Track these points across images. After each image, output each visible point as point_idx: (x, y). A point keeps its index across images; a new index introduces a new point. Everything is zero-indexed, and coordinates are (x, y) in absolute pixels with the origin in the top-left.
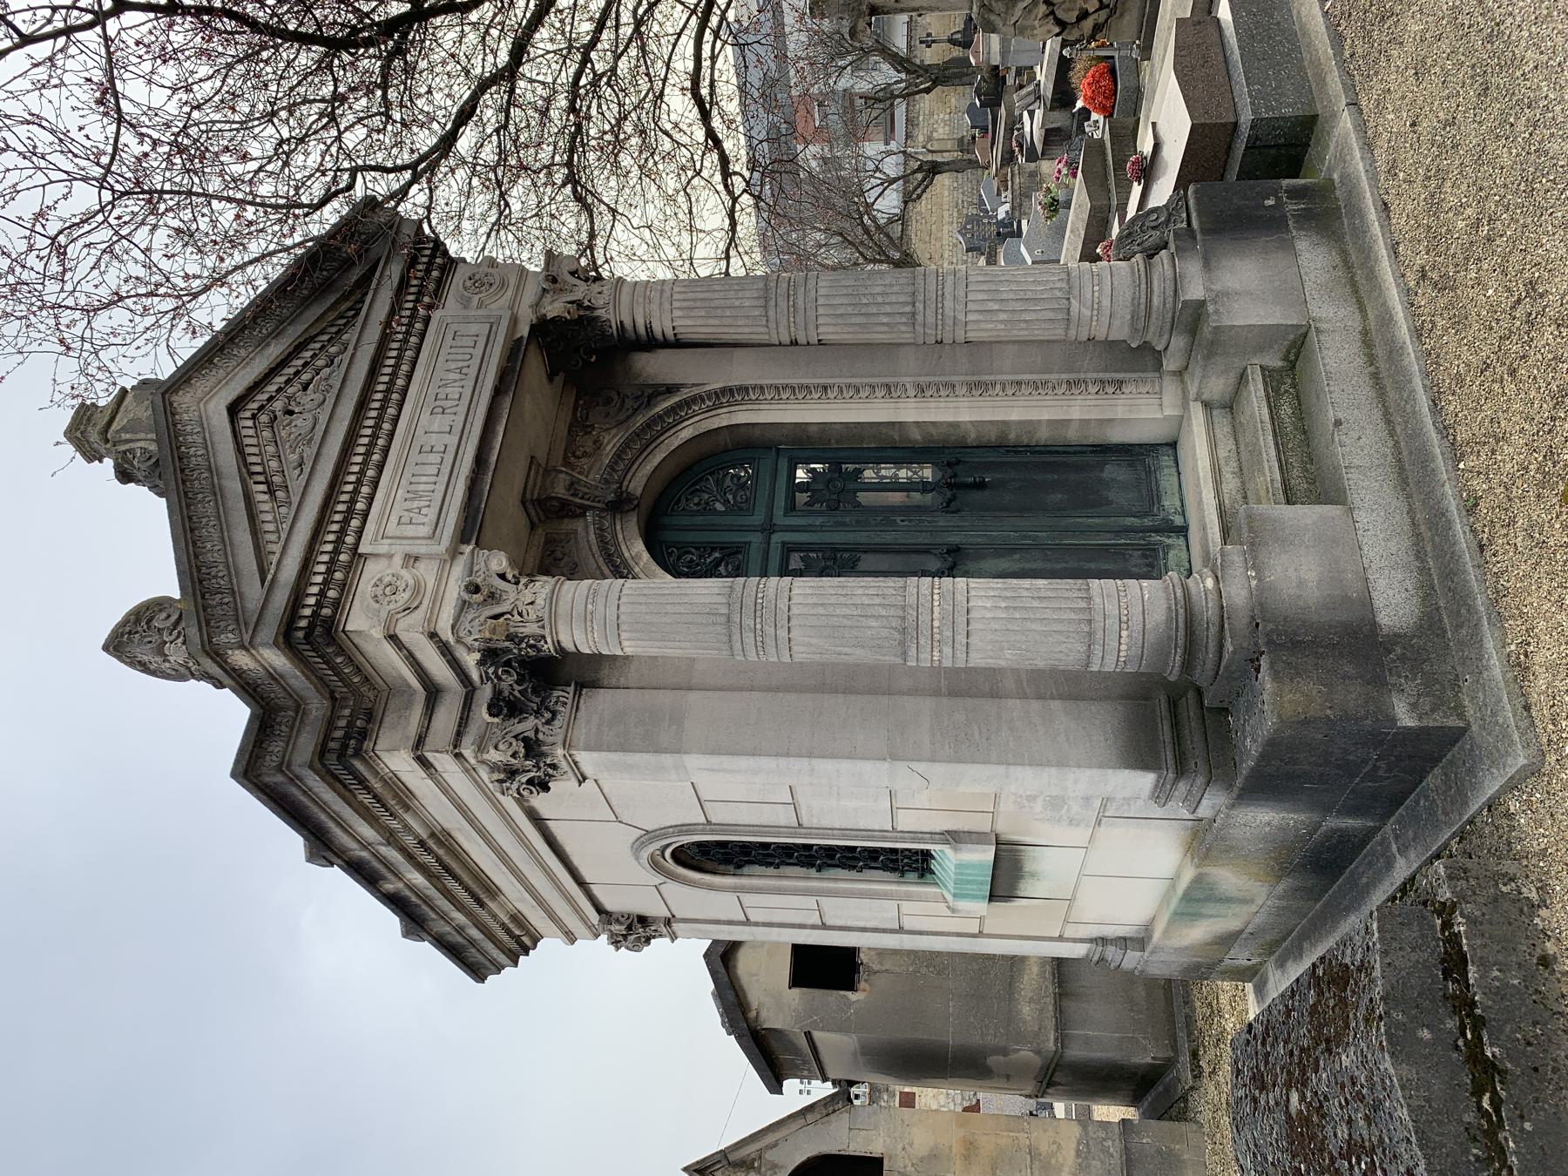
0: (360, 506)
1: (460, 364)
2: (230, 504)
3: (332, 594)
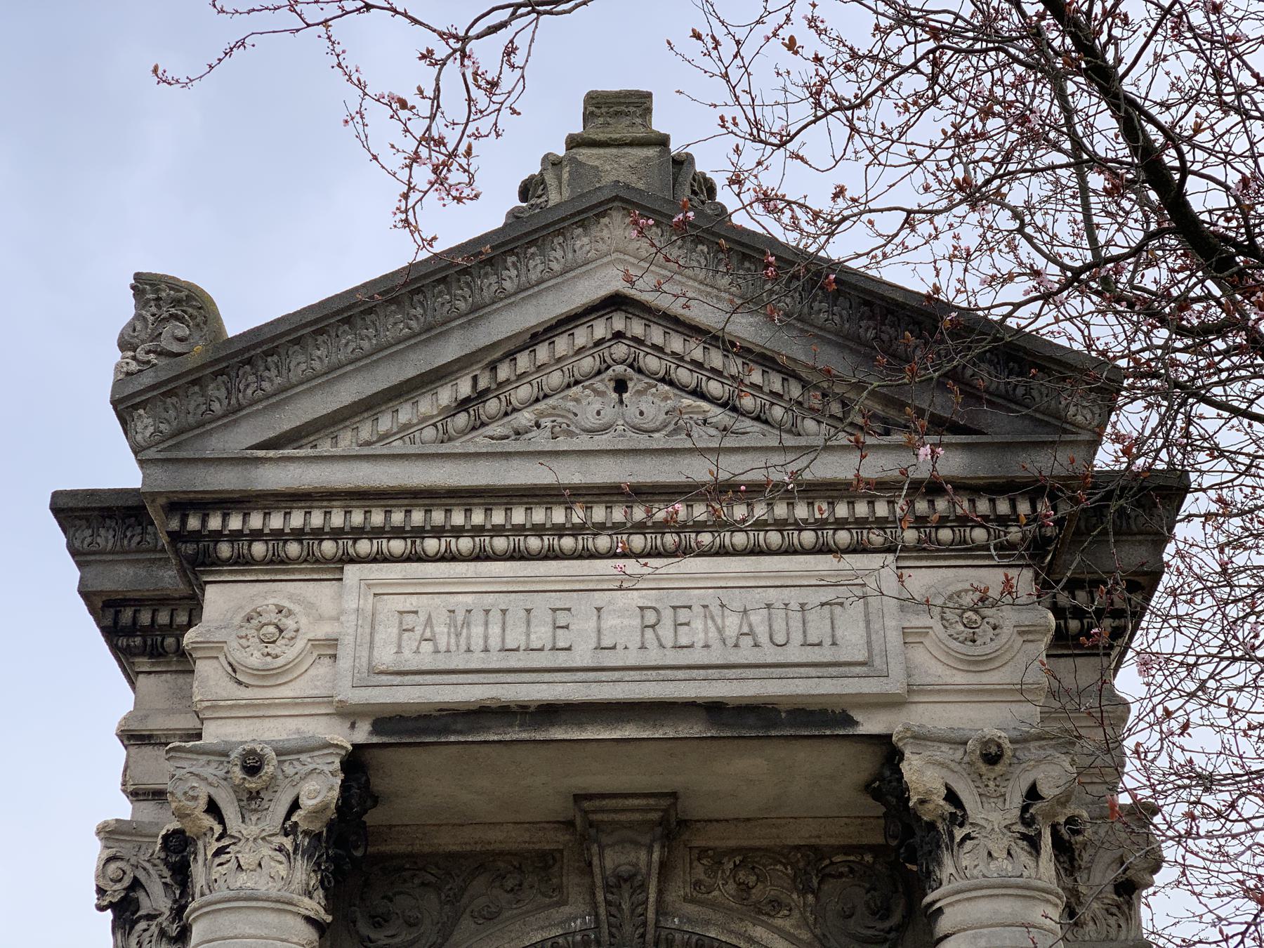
0: (431, 545)
2: (412, 356)
3: (259, 549)
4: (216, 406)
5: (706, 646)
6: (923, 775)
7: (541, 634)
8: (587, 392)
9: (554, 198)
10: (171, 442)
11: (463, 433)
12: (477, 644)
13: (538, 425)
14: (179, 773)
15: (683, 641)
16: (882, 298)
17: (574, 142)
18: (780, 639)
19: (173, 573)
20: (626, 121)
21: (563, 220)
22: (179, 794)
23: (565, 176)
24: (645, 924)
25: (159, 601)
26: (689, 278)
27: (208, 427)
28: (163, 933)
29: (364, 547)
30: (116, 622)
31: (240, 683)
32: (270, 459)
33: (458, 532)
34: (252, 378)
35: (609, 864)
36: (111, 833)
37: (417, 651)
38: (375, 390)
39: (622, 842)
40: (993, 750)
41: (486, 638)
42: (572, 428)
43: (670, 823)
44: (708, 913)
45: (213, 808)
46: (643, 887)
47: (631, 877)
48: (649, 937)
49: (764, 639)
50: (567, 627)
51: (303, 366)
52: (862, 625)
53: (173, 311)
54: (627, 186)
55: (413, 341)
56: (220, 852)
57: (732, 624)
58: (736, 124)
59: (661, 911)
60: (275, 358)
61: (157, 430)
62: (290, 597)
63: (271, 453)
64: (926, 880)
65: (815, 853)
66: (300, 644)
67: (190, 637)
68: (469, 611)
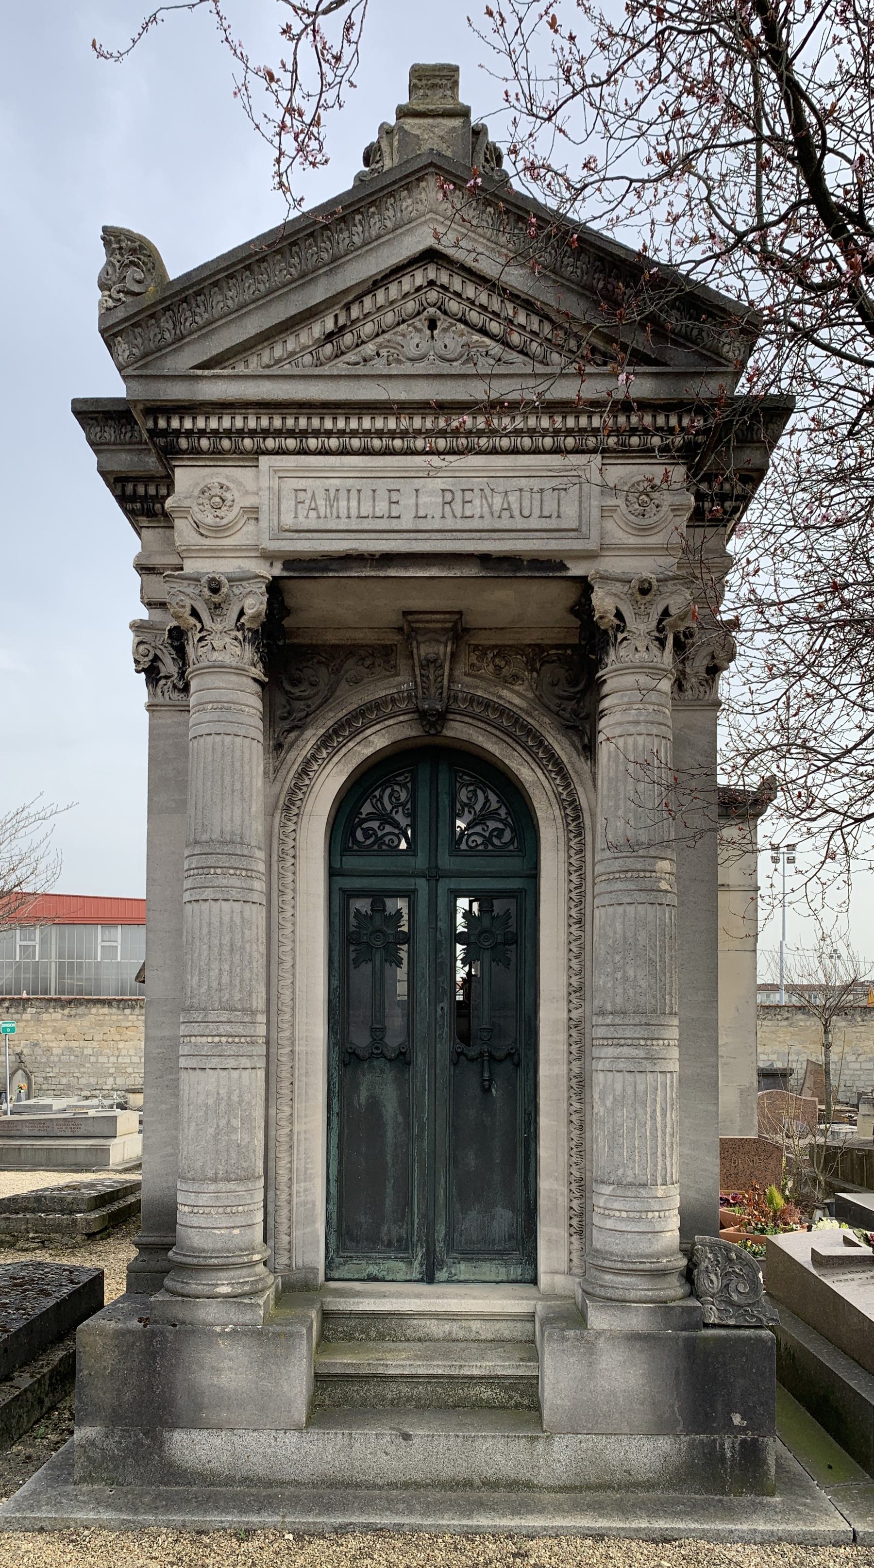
0: (312, 443)
1: (515, 507)
2: (294, 297)
3: (204, 443)
4: (167, 335)
5: (482, 517)
6: (603, 601)
7: (382, 507)
8: (410, 329)
9: (388, 164)
10: (141, 363)
11: (330, 359)
12: (343, 512)
13: (378, 355)
14: (173, 591)
15: (468, 513)
16: (611, 254)
17: (403, 113)
18: (526, 513)
19: (155, 459)
20: (440, 93)
21: (394, 183)
22: (174, 603)
23: (396, 143)
24: (442, 687)
25: (148, 479)
26: (480, 235)
27: (164, 352)
28: (175, 687)
29: (270, 443)
30: (123, 491)
31: (202, 535)
32: (206, 377)
33: (329, 434)
34: (188, 314)
35: (422, 653)
36: (138, 627)
37: (307, 517)
38: (270, 325)
39: (429, 641)
40: (646, 586)
41: (348, 509)
42: (400, 357)
43: (458, 629)
44: (478, 682)
45: (195, 613)
46: (441, 666)
47: (435, 661)
48: (444, 695)
49: (516, 513)
50: (397, 502)
51: (221, 305)
52: (577, 503)
53: (131, 258)
54: (439, 154)
55: (293, 285)
56: (201, 639)
57: (498, 502)
58: (518, 100)
59: (451, 680)
60: (203, 297)
61: (132, 354)
62: (227, 477)
63: (206, 372)
64: (599, 663)
65: (539, 648)
66: (236, 509)
67: (169, 503)
68: (338, 490)
